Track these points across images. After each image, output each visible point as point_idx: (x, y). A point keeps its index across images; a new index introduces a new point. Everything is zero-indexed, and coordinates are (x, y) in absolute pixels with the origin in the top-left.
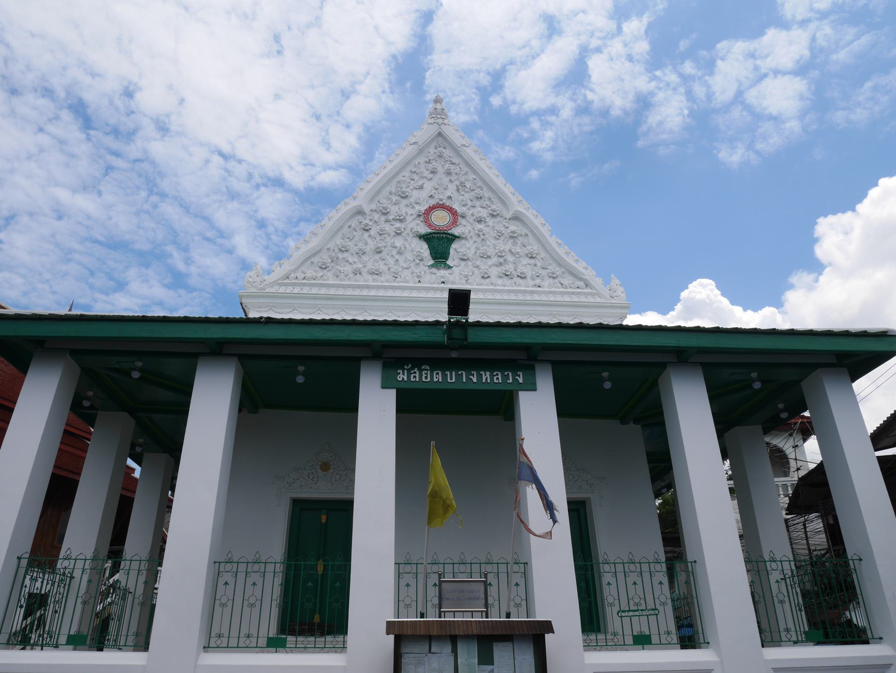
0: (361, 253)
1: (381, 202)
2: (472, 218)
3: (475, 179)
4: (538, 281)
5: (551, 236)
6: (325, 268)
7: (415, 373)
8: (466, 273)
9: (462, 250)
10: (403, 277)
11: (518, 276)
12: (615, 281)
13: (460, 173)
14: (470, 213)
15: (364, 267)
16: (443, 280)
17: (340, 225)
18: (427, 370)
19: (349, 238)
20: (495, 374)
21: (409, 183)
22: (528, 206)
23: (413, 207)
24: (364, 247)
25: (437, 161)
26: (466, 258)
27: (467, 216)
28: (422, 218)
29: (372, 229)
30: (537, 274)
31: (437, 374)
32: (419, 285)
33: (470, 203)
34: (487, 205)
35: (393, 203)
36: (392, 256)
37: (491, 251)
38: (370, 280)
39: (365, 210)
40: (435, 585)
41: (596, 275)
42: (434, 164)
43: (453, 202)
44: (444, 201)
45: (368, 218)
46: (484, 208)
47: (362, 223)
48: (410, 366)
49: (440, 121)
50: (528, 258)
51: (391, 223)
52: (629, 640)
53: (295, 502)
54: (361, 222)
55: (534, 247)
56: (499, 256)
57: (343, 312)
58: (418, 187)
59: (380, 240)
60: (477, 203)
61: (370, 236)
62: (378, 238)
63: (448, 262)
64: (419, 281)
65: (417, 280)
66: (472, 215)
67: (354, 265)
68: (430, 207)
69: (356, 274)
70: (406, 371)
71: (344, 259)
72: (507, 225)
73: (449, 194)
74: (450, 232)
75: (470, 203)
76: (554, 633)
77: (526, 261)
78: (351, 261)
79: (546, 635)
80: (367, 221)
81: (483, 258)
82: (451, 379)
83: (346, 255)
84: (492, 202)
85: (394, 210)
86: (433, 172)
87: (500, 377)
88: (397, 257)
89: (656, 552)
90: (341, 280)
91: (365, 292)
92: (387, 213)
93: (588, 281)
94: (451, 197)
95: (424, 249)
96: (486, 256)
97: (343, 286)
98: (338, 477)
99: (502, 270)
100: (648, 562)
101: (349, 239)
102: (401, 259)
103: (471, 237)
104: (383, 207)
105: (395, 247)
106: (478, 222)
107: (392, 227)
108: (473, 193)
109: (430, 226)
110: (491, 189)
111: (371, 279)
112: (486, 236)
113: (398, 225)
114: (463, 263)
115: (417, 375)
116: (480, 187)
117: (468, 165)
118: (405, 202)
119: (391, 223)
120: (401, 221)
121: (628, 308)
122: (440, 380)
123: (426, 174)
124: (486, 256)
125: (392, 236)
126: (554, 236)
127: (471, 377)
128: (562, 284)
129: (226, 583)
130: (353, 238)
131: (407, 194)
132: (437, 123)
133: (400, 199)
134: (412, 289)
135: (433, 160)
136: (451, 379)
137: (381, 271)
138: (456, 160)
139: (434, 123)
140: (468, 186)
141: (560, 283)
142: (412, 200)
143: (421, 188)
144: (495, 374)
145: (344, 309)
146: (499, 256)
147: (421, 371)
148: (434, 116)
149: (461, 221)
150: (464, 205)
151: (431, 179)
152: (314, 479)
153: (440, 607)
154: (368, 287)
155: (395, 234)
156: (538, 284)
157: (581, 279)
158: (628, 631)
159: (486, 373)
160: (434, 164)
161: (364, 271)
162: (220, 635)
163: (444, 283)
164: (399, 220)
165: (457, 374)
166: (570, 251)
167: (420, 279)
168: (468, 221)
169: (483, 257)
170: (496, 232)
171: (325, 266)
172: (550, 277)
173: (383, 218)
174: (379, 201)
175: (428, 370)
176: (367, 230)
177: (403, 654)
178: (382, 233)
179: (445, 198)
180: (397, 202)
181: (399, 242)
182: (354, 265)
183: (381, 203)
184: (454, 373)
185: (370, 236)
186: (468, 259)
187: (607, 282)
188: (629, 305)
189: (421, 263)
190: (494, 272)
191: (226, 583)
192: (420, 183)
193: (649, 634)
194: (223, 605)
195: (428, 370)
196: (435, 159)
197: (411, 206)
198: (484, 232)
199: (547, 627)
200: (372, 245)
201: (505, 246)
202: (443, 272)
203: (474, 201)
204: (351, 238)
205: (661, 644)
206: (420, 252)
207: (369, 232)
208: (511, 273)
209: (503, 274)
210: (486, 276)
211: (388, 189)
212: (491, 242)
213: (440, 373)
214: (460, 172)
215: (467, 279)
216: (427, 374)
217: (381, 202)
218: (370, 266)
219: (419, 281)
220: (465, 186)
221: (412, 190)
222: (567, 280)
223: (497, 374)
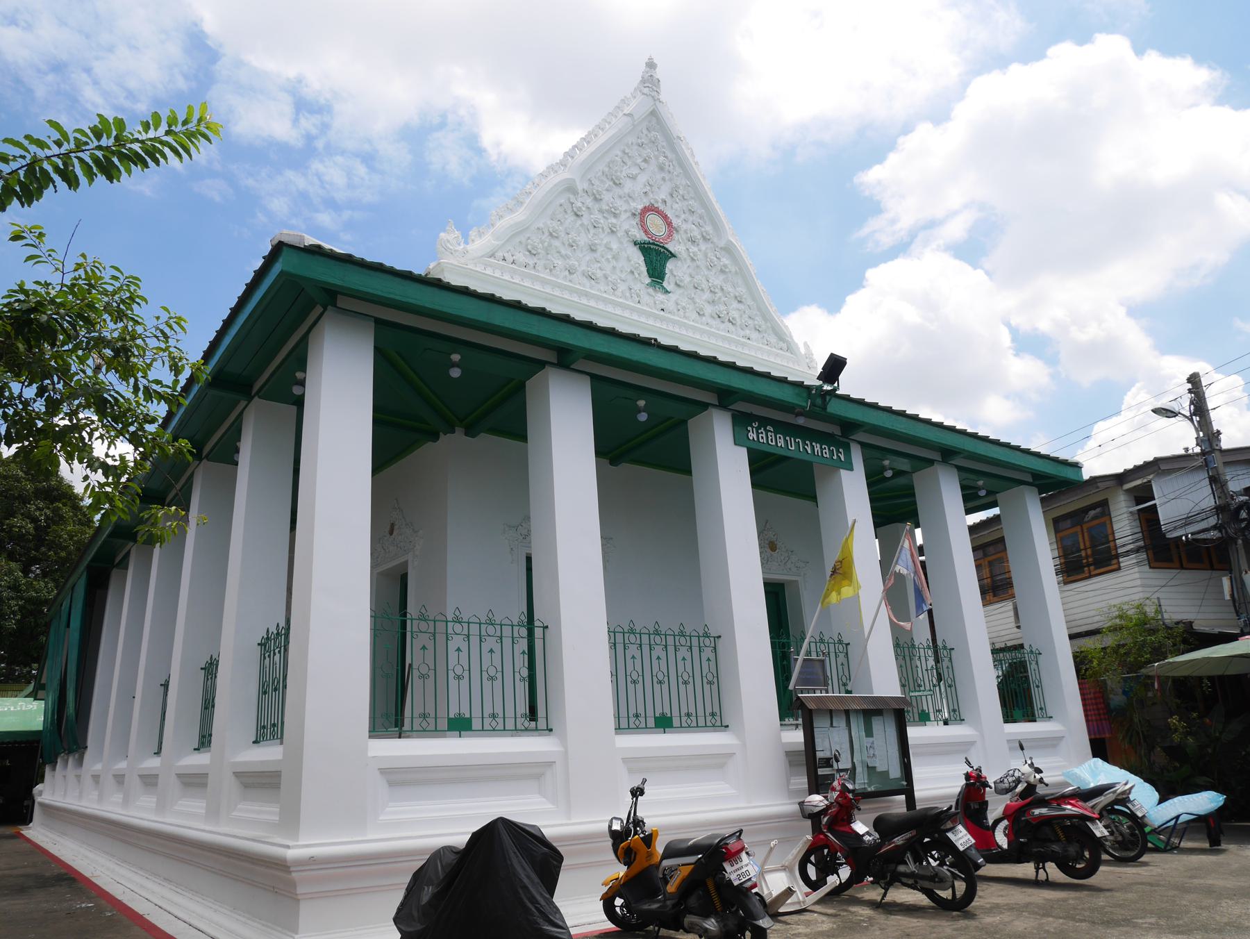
1: (593, 182)
3: (689, 186)
4: (748, 332)
8: (684, 304)
11: (729, 321)
18: (771, 432)
19: (559, 221)
23: (627, 202)
28: (637, 219)
31: (780, 438)
32: (638, 306)
33: (683, 216)
38: (587, 286)
40: (524, 652)
44: (660, 204)
45: (580, 199)
49: (654, 94)
50: (737, 302)
55: (741, 290)
61: (582, 225)
62: (592, 231)
63: (665, 284)
68: (645, 208)
70: (754, 429)
74: (666, 246)
75: (683, 216)
80: (579, 204)
82: (791, 447)
83: (556, 243)
84: (705, 223)
85: (607, 197)
86: (645, 161)
89: (706, 625)
90: (554, 276)
92: (601, 200)
94: (665, 202)
95: (638, 258)
99: (716, 309)
100: (697, 635)
101: (559, 222)
105: (611, 249)
109: (646, 232)
113: (614, 221)
115: (764, 436)
118: (617, 191)
120: (615, 215)
125: (606, 232)
132: (653, 97)
133: (614, 186)
136: (791, 447)
139: (650, 95)
140: (681, 193)
142: (626, 191)
143: (634, 178)
146: (711, 291)
147: (767, 431)
148: (650, 86)
149: (675, 236)
150: (677, 216)
154: (587, 294)
155: (610, 231)
165: (795, 441)
170: (709, 260)
172: (756, 329)
173: (597, 206)
184: (792, 439)
186: (683, 287)
190: (709, 309)
192: (635, 171)
197: (625, 199)
200: (583, 240)
201: (717, 281)
202: (660, 297)
207: (581, 220)
213: (782, 437)
216: (771, 436)
218: (584, 268)
219: (639, 302)
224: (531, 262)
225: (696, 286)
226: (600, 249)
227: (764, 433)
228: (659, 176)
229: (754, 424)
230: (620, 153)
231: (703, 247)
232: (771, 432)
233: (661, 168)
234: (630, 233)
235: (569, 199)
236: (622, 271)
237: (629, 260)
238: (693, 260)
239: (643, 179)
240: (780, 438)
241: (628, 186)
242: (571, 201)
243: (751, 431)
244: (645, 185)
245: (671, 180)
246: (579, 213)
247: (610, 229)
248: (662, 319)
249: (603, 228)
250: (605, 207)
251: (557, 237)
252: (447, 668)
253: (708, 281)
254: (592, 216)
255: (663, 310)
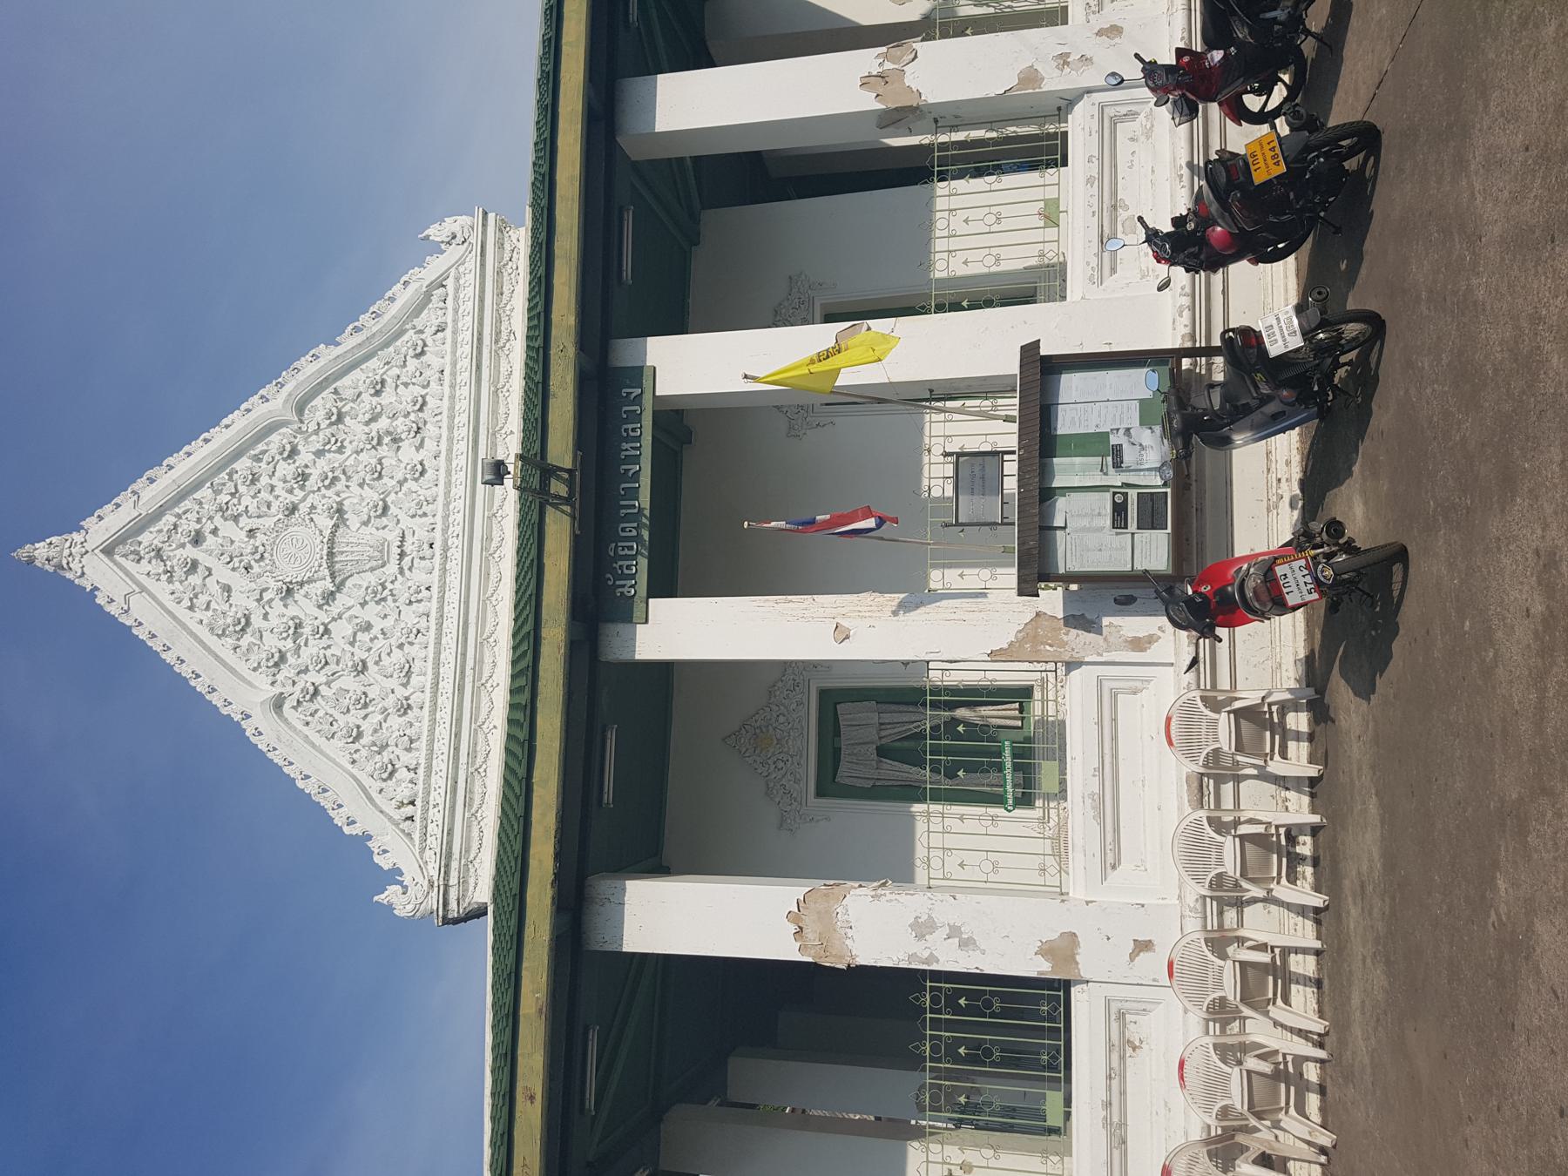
0: (364, 703)
1: (256, 665)
2: (297, 491)
3: (212, 484)
5: (338, 344)
6: (393, 765)
7: (621, 567)
9: (366, 510)
10: (417, 620)
11: (421, 409)
12: (436, 232)
13: (198, 513)
14: (284, 494)
15: (393, 692)
16: (426, 546)
17: (302, 742)
18: (616, 547)
19: (331, 724)
20: (625, 435)
21: (215, 610)
22: (274, 383)
24: (351, 694)
25: (169, 557)
26: (381, 503)
27: (292, 502)
29: (313, 681)
30: (418, 374)
31: (623, 530)
32: (435, 589)
33: (264, 495)
34: (269, 463)
35: (258, 642)
36: (372, 640)
37: (368, 458)
39: (273, 694)
41: (419, 267)
42: (175, 562)
43: (262, 527)
45: (289, 689)
46: (275, 468)
47: (301, 700)
48: (609, 576)
51: (302, 644)
52: (1051, 233)
53: (820, 793)
54: (298, 700)
56: (379, 443)
57: (485, 727)
58: (226, 594)
59: (338, 664)
60: (264, 480)
61: (328, 684)
64: (428, 589)
65: (425, 593)
66: (291, 491)
67: (390, 711)
69: (409, 706)
70: (618, 583)
71: (375, 731)
72: (313, 427)
73: (244, 533)
75: (264, 495)
76: (1039, 340)
77: (388, 397)
78: (380, 717)
79: (1041, 354)
81: (383, 473)
85: (272, 643)
87: (630, 426)
88: (375, 631)
91: (447, 686)
92: (280, 651)
93: (432, 283)
94: (250, 531)
96: (379, 467)
97: (432, 731)
98: (782, 719)
102: (378, 625)
103: (338, 495)
104: (268, 660)
106: (305, 481)
107: (311, 642)
108: (242, 489)
110: (237, 455)
111: (422, 678)
112: (336, 465)
113: (307, 630)
114: (393, 510)
116: (230, 475)
117: (182, 496)
118: (257, 621)
119: (302, 644)
120: (298, 626)
121: (486, 213)
122: (635, 525)
123: (195, 580)
124: (379, 467)
126: (338, 339)
127: (632, 472)
128: (438, 331)
129: (961, 865)
130: (331, 716)
131: (239, 615)
134: (442, 599)
135: (165, 566)
137: (403, 660)
138: (169, 519)
141: (435, 334)
143: (227, 589)
144: (625, 435)
145: (478, 724)
151: (209, 570)
152: (785, 759)
153: (997, 524)
155: (326, 636)
156: (438, 375)
157: (428, 297)
158: (1038, 235)
159: (624, 448)
160: (175, 562)
161: (401, 692)
162: (1041, 870)
163: (433, 544)
164: (296, 628)
166: (370, 312)
167: (422, 588)
168: (304, 499)
169: (380, 473)
170: (327, 447)
171: (389, 766)
173: (291, 660)
174: (255, 670)
175: (616, 545)
176: (316, 692)
177: (1067, 570)
178: (323, 661)
179: (252, 541)
180: (258, 634)
181: (342, 630)
182: (390, 711)
183: (259, 663)
184: (623, 503)
185: (328, 684)
186: (384, 500)
187: (436, 249)
188: (481, 209)
189: (390, 586)
191: (961, 865)
192: (215, 588)
193: (1043, 202)
194: (995, 866)
195: (616, 545)
196: (162, 560)
198: (326, 469)
199: (1030, 352)
200: (349, 682)
201: (355, 429)
203: (259, 485)
204: (331, 719)
205: (1058, 184)
206: (367, 589)
208: (414, 422)
209: (415, 437)
210: (419, 468)
211: (227, 655)
212: (351, 455)
214: (195, 513)
215: (425, 503)
217: (256, 665)
218: (393, 683)
219: (428, 589)
220: (227, 503)
221: (231, 605)
222: (429, 318)
223: (626, 430)
224: (402, 774)
225: (376, 475)
226: (360, 654)
227: (620, 563)
228: (210, 541)
229: (610, 583)
230: (198, 615)
231: (305, 457)
232: (616, 547)
233: (197, 540)
234: (321, 602)
235: (294, 707)
236: (385, 616)
237: (363, 604)
238: (335, 479)
239: (223, 574)
240: (623, 530)
241: (243, 601)
242: (295, 704)
243: (620, 590)
244: (234, 569)
245: (211, 518)
246: (311, 689)
247: (323, 635)
248: (446, 549)
249: (323, 648)
250: (289, 644)
251: (358, 727)
252: (984, 1167)
253: (362, 450)
254: (310, 668)
255: (431, 546)
